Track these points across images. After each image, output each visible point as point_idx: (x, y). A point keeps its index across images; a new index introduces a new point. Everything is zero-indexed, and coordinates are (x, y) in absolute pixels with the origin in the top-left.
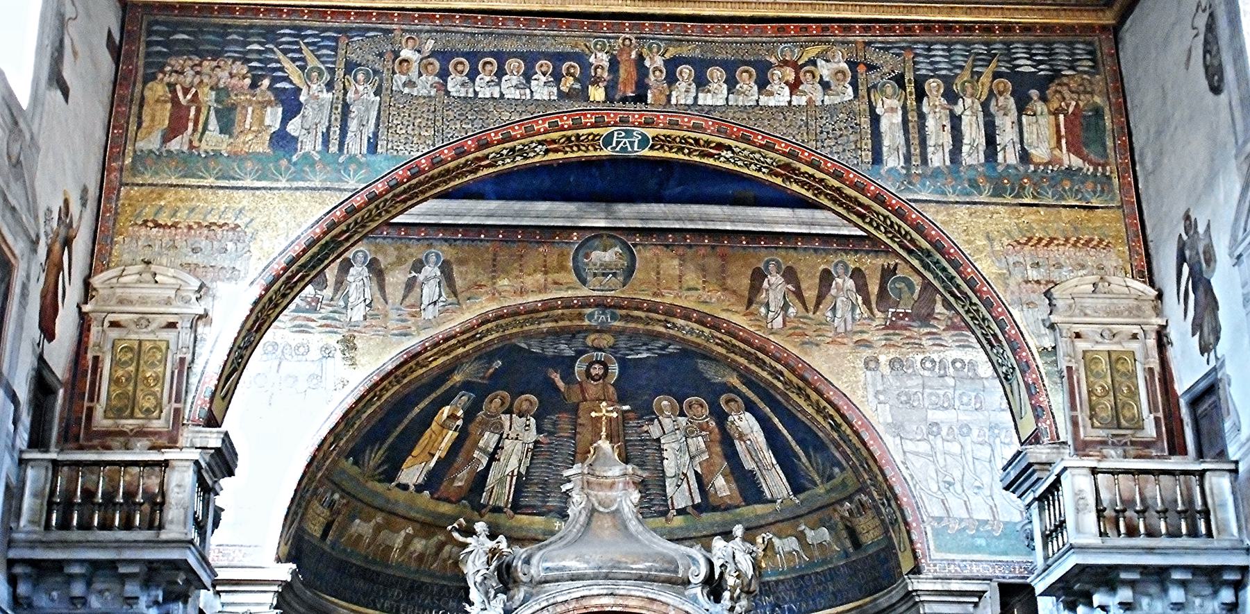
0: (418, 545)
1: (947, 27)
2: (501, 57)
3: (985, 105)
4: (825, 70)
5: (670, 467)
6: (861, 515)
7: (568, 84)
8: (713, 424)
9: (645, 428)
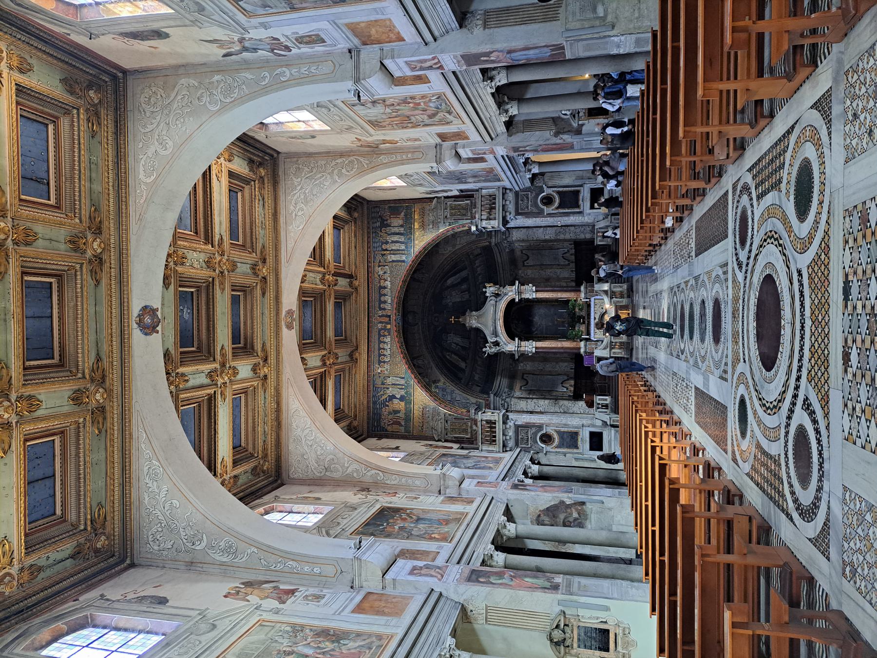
0: (479, 363)
1: (368, 242)
2: (380, 349)
3: (389, 235)
4: (381, 273)
5: (458, 300)
7: (386, 333)
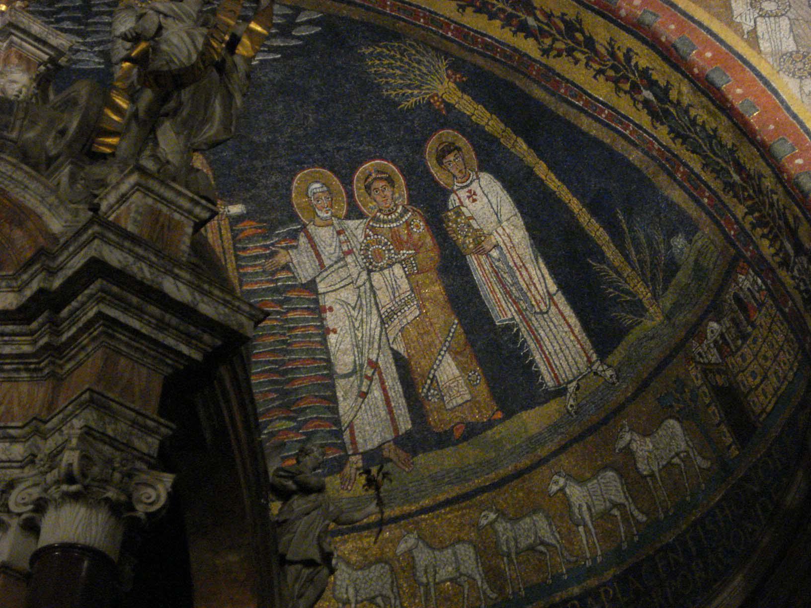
6: (744, 337)
8: (420, 227)
9: (282, 258)
